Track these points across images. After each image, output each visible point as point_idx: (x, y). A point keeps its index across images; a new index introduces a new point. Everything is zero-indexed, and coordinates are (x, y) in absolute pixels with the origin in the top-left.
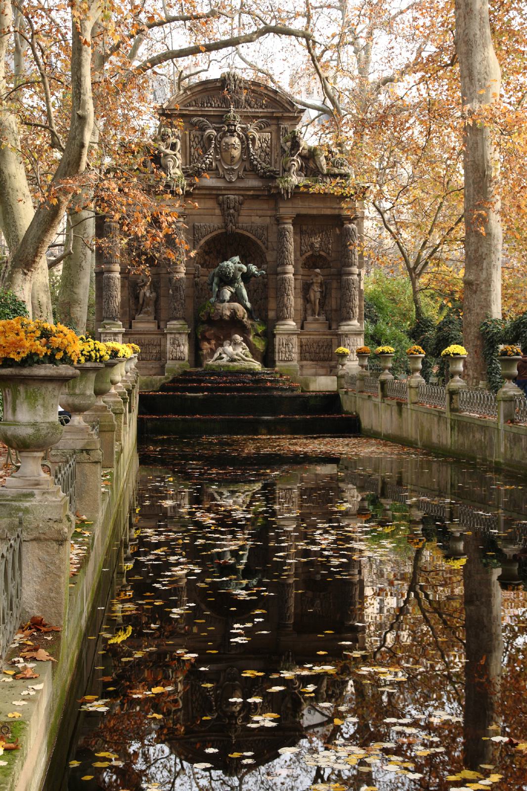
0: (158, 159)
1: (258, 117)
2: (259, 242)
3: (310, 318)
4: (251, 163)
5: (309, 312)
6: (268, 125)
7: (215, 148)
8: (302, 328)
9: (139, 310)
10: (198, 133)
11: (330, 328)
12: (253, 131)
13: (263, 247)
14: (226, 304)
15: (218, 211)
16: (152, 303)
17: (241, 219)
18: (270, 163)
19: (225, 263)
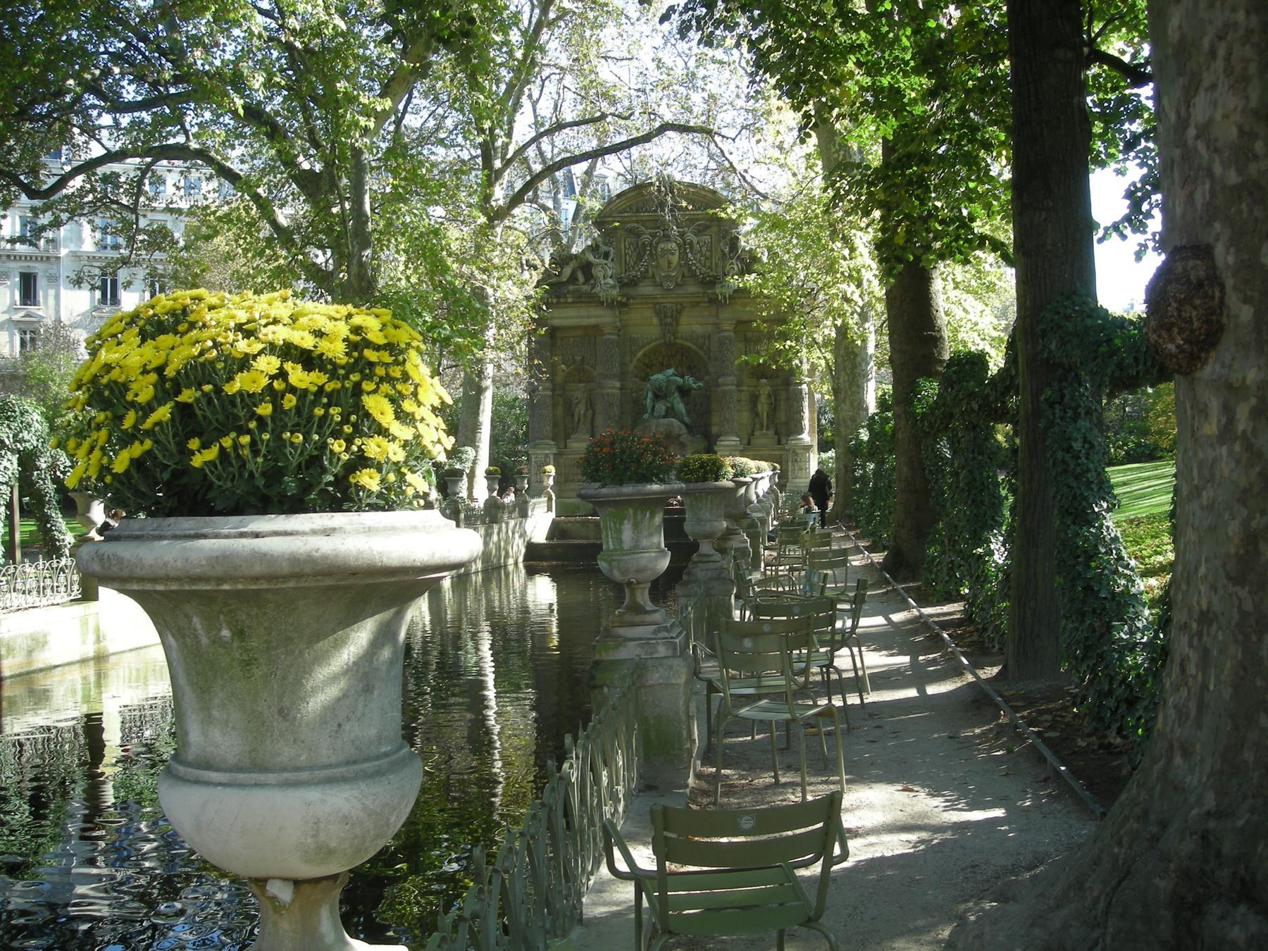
0: (587, 268)
1: (698, 220)
2: (701, 353)
3: (757, 433)
4: (690, 269)
5: (758, 426)
6: (707, 227)
7: (651, 254)
8: (749, 443)
9: (575, 430)
10: (633, 240)
11: (779, 443)
12: (690, 236)
13: (705, 357)
14: (662, 421)
15: (655, 321)
16: (589, 420)
17: (681, 328)
18: (710, 268)
19: (655, 377)
